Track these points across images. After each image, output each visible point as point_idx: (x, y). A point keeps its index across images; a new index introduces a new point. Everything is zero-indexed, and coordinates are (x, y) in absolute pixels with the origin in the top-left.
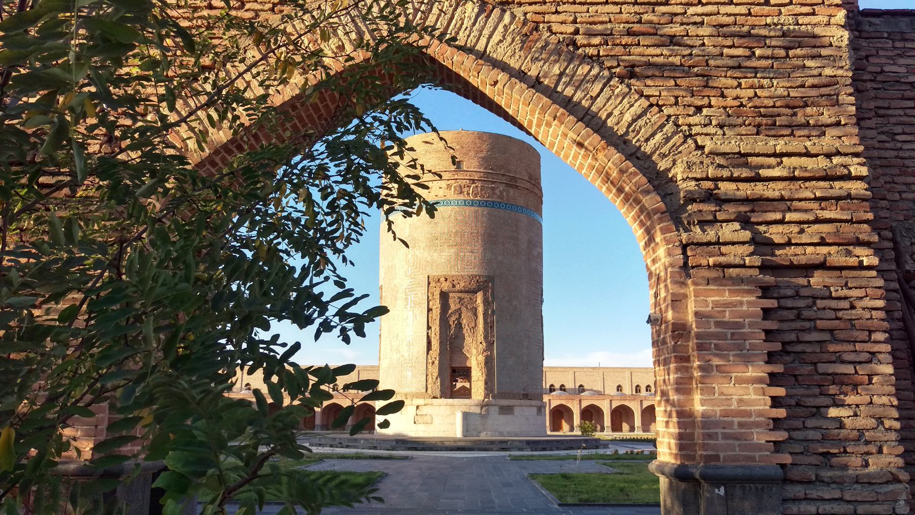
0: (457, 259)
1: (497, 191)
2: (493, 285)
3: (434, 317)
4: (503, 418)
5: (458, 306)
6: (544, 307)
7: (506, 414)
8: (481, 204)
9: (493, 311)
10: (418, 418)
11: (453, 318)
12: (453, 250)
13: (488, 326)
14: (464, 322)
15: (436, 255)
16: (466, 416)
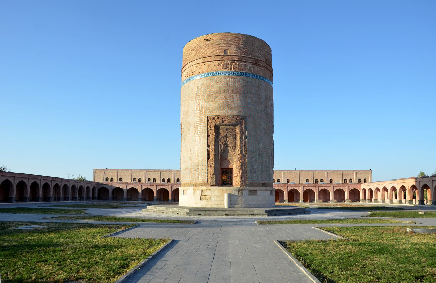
1: (248, 67)
2: (246, 121)
3: (211, 140)
4: (251, 197)
5: (225, 134)
6: (274, 135)
7: (253, 195)
9: (246, 136)
10: (203, 197)
11: (222, 141)
12: (222, 101)
13: (243, 145)
14: (229, 143)
16: (230, 196)
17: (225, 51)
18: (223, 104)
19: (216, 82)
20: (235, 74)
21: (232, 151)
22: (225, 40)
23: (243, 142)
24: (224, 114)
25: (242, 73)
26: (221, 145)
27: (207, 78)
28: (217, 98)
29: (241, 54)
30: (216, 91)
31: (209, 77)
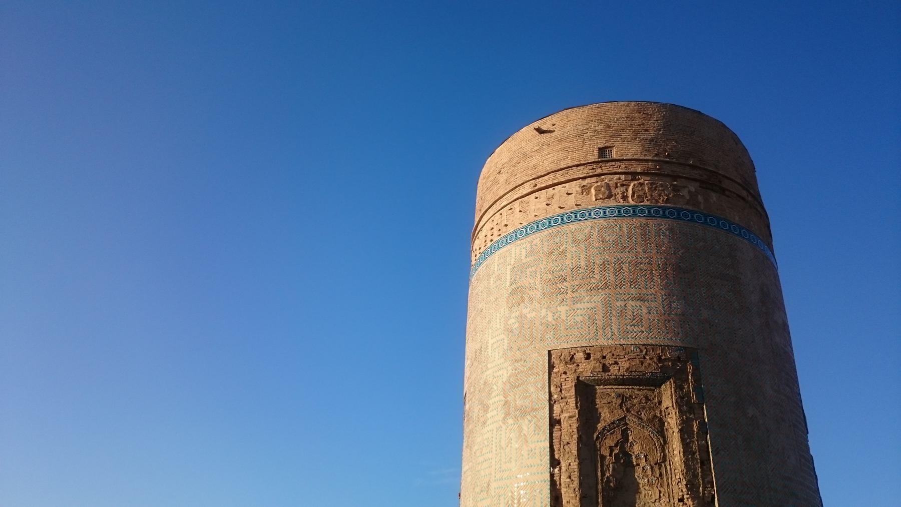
0: (607, 315)
1: (684, 193)
2: (696, 369)
3: (566, 439)
5: (619, 414)
8: (652, 213)
9: (702, 424)
11: (610, 441)
12: (598, 298)
15: (562, 309)
17: (602, 151)
18: (600, 305)
19: (576, 242)
20: (642, 211)
21: (650, 484)
22: (600, 121)
23: (695, 447)
24: (611, 342)
25: (664, 209)
26: (603, 458)
27: (545, 233)
28: (582, 291)
29: (656, 155)
30: (578, 267)
31: (550, 230)
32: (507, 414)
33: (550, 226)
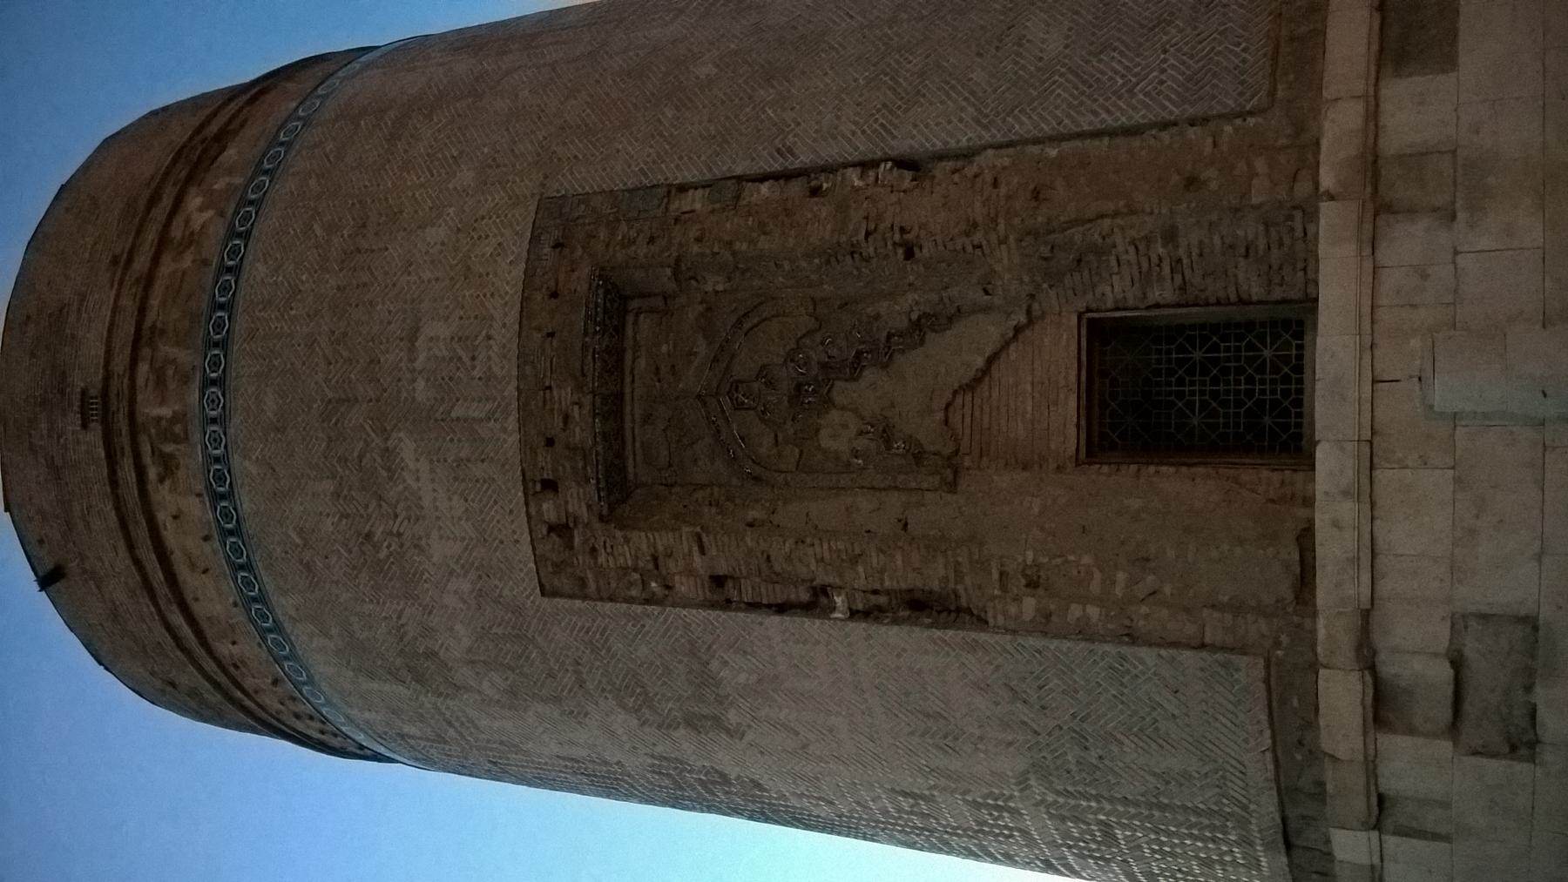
24: (512, 423)
31: (260, 566)
32: (718, 722)
33: (248, 567)
